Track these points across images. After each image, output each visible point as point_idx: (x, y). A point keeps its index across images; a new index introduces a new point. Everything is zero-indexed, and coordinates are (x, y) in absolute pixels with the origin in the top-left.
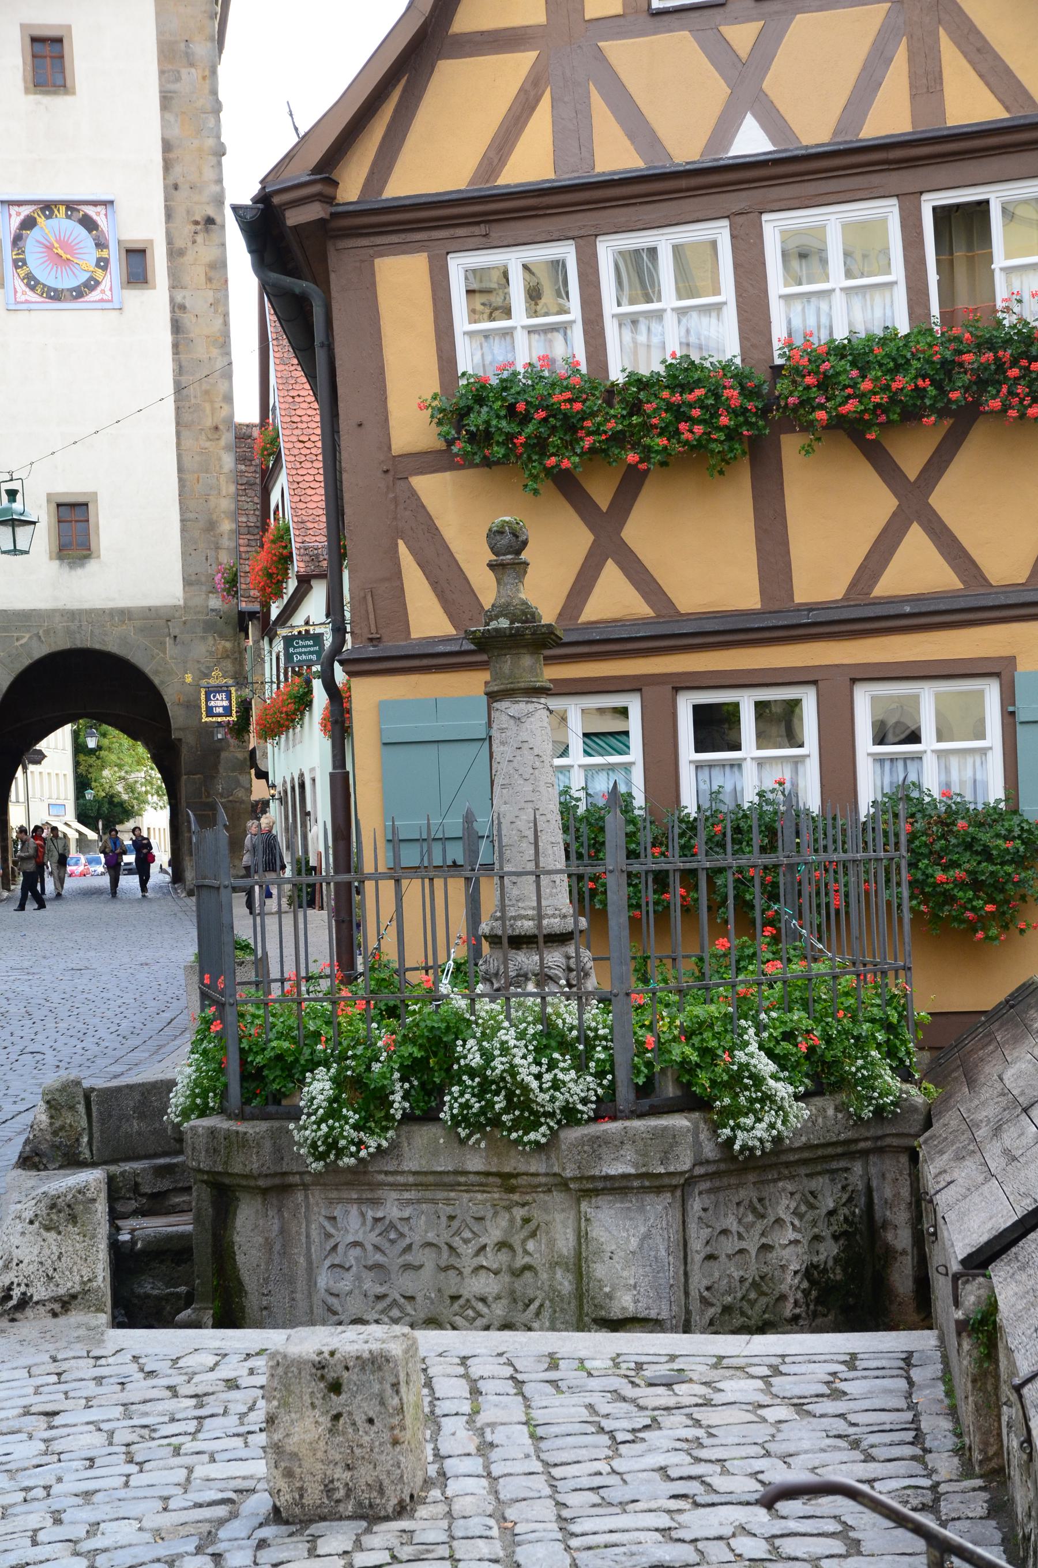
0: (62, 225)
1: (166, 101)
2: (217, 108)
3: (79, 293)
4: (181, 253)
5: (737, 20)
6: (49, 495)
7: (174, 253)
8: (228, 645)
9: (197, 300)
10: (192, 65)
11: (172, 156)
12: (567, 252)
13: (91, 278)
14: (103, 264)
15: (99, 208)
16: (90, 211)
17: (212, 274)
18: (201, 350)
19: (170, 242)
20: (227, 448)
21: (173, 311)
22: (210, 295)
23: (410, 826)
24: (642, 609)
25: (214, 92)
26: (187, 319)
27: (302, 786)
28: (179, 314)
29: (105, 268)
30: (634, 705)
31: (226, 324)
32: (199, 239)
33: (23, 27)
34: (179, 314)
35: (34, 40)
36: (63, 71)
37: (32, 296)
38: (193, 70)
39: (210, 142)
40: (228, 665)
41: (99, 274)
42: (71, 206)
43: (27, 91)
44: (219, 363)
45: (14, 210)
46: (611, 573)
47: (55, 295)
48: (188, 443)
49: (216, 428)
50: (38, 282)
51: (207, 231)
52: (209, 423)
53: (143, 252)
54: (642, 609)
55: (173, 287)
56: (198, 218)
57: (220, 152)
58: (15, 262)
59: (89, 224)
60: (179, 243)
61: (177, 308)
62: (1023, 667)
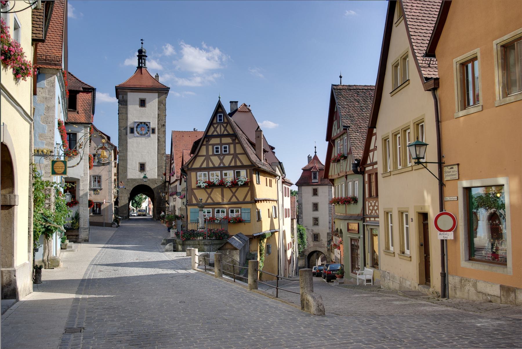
1: (158, 108)
2: (166, 110)
4: (160, 129)
6: (139, 163)
9: (162, 136)
12: (207, 173)
16: (147, 123)
20: (165, 157)
24: (212, 202)
25: (165, 107)
27: (175, 206)
30: (211, 210)
31: (165, 139)
33: (139, 98)
36: (145, 104)
37: (138, 135)
41: (148, 132)
42: (145, 123)
44: (164, 145)
46: (210, 198)
47: (141, 135)
48: (159, 156)
53: (154, 129)
54: (212, 202)
57: (165, 116)
60: (159, 128)
61: (158, 137)
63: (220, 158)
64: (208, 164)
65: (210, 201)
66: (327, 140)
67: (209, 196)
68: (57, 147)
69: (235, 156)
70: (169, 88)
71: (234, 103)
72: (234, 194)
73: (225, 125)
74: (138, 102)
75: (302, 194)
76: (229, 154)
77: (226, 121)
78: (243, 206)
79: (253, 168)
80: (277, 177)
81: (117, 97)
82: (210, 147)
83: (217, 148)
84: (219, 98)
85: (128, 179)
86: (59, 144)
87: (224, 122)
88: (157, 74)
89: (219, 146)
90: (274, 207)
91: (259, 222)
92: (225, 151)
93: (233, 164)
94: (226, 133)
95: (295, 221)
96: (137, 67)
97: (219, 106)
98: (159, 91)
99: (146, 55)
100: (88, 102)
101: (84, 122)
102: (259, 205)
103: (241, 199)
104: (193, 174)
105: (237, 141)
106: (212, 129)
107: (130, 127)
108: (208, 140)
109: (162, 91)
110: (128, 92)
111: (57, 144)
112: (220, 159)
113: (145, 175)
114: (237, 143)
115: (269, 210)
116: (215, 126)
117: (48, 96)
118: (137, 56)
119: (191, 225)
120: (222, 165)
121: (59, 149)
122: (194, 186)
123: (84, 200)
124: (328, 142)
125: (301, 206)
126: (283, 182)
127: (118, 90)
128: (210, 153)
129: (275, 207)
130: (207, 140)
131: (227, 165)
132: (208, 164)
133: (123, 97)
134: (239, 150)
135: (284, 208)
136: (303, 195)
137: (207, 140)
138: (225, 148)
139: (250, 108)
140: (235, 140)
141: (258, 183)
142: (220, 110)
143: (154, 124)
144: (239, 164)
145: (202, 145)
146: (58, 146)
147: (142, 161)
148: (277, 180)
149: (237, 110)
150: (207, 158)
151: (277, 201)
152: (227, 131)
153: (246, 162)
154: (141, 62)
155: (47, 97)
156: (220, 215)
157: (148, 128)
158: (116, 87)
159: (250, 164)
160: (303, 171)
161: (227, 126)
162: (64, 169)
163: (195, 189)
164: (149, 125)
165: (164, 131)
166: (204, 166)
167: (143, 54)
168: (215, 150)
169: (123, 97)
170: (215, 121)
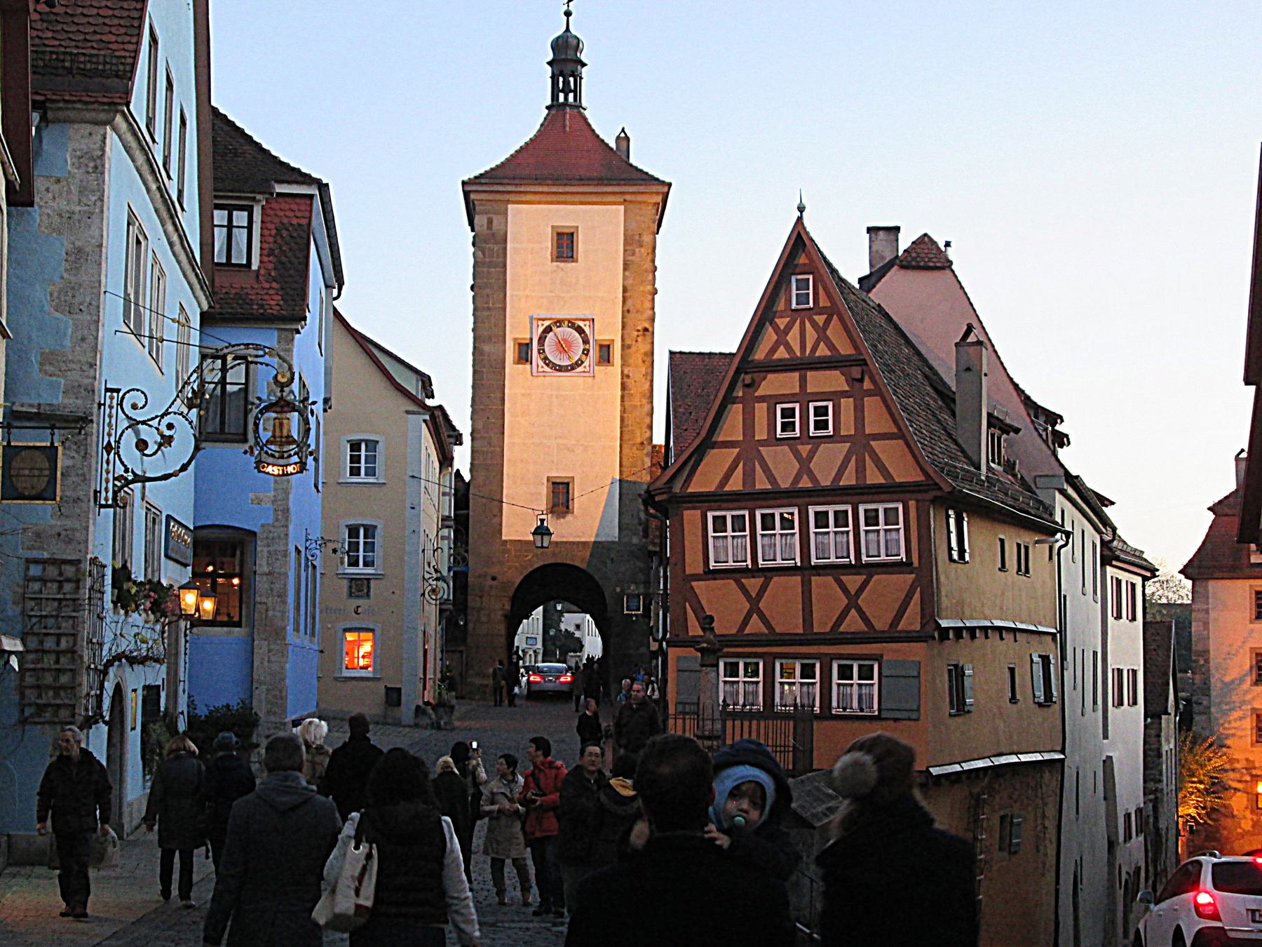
0: (565, 331)
2: (655, 269)
3: (573, 367)
4: (629, 347)
5: (802, 444)
7: (625, 347)
8: (642, 565)
9: (637, 373)
10: (641, 246)
11: (627, 294)
13: (579, 359)
14: (586, 352)
15: (587, 323)
16: (581, 324)
17: (645, 358)
18: (636, 401)
19: (623, 340)
20: (647, 455)
21: (622, 378)
22: (643, 370)
23: (682, 698)
25: (653, 261)
26: (629, 382)
28: (625, 380)
29: (587, 355)
31: (652, 386)
32: (640, 339)
33: (553, 227)
34: (625, 380)
35: (558, 234)
38: (642, 250)
39: (649, 288)
40: (641, 577)
42: (572, 324)
43: (552, 261)
45: (540, 323)
47: (561, 369)
49: (642, 443)
50: (550, 361)
51: (644, 335)
52: (639, 440)
55: (623, 365)
56: (640, 328)
58: (539, 350)
59: (580, 330)
60: (628, 342)
62: (885, 658)
63: (798, 451)
64: (749, 476)
65: (755, 626)
66: (1247, 382)
67: (755, 609)
68: (108, 402)
69: (861, 443)
70: (670, 185)
71: (881, 233)
72: (853, 601)
73: (820, 319)
74: (548, 244)
75: (1207, 611)
76: (835, 438)
77: (824, 302)
78: (890, 651)
79: (931, 494)
80: (1058, 536)
81: (471, 223)
82: (761, 409)
83: (788, 413)
84: (801, 209)
85: (506, 541)
86: (118, 391)
87: (817, 309)
88: (623, 130)
89: (797, 406)
90: (1036, 659)
91: (959, 720)
92: (821, 425)
93: (848, 480)
94: (823, 351)
95: (1169, 723)
96: (547, 108)
97: (799, 242)
98: (628, 197)
99: (584, 58)
100: (295, 235)
101: (275, 311)
102: (961, 653)
103: (881, 624)
104: (691, 516)
105: (867, 384)
106: (770, 336)
107: (515, 339)
108: (753, 380)
109: (639, 198)
110: (508, 202)
111: (107, 390)
112: (797, 454)
113: (542, 521)
114: (869, 393)
115: (1012, 670)
116: (782, 322)
117: (78, 208)
118: (550, 63)
119: (680, 722)
120: (805, 483)
121: (114, 411)
122: (693, 565)
123: (270, 613)
124: (1253, 388)
125: (1202, 662)
126: (1106, 561)
127: (472, 196)
128: (761, 434)
129: (1045, 660)
130: (748, 379)
131: (826, 482)
132: (749, 476)
133: (490, 222)
134: (876, 420)
135: (1112, 665)
136: (1212, 615)
137: (748, 381)
138: (821, 411)
139: (951, 253)
140: (861, 380)
141: (955, 555)
142: (802, 260)
143: (609, 329)
144: (874, 477)
145: (728, 400)
146: (112, 398)
147: (560, 473)
148: (1057, 545)
149: (895, 262)
150: (749, 451)
151: (1054, 635)
152: (831, 346)
153: (904, 472)
154: (561, 85)
155: (73, 213)
156: (855, 688)
157: (586, 341)
158: (464, 183)
159: (920, 478)
160: (1211, 516)
161: (827, 322)
162: (46, 479)
163: (697, 578)
164: (587, 330)
165: (645, 354)
166: (735, 484)
167: (570, 55)
168: (779, 421)
169: (490, 222)
170: (781, 306)
